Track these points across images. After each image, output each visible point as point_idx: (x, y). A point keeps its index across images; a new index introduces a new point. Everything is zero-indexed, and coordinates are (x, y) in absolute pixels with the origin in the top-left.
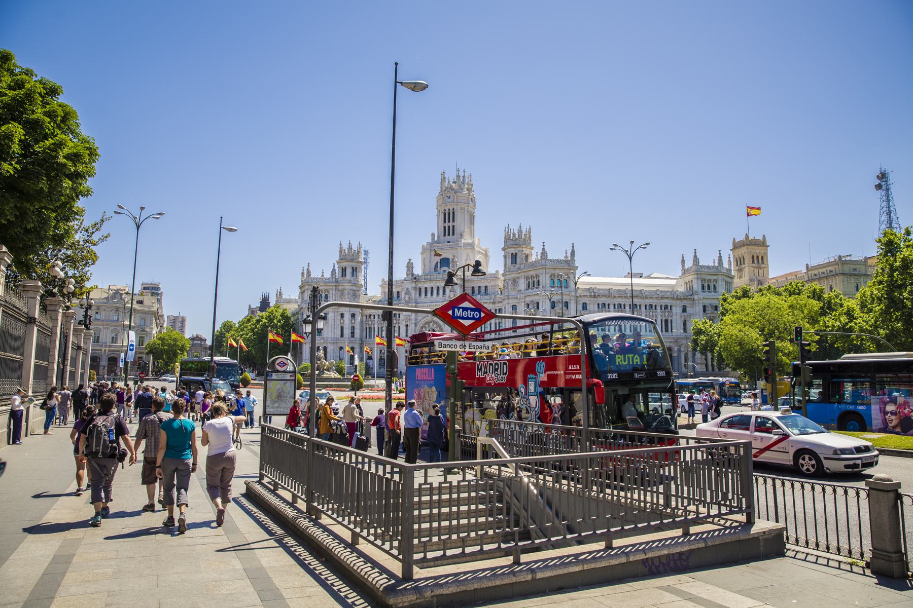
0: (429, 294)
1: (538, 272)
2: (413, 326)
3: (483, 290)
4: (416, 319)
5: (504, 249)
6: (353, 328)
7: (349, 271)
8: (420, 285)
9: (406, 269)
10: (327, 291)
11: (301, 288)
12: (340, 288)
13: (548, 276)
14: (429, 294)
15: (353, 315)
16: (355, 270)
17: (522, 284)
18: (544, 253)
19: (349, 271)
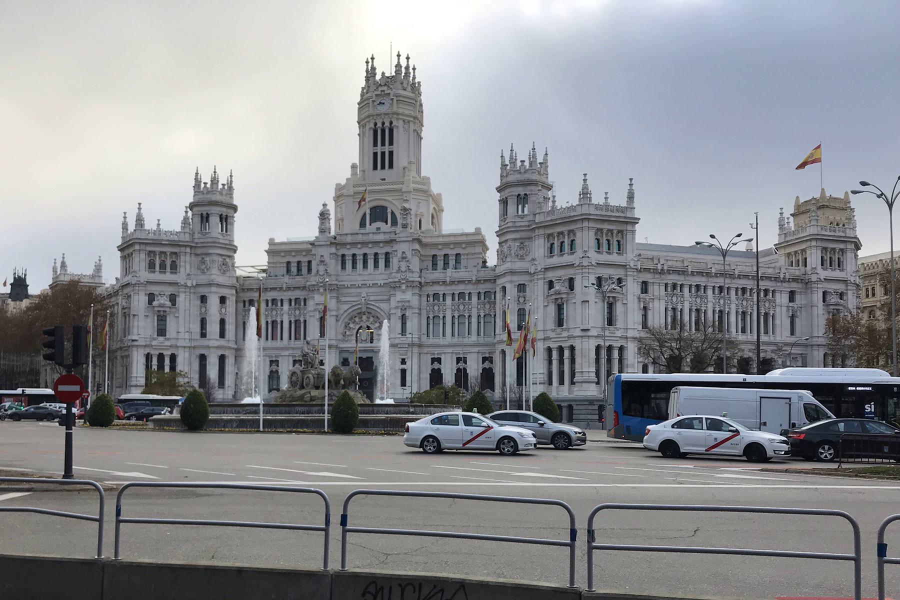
0: (360, 265)
1: (572, 227)
2: (333, 319)
3: (452, 262)
4: (338, 309)
5: (499, 190)
6: (222, 322)
7: (215, 220)
8: (343, 251)
9: (317, 222)
11: (121, 249)
12: (199, 251)
13: (592, 234)
14: (360, 265)
15: (223, 300)
16: (226, 221)
17: (539, 247)
18: (585, 194)
19: (215, 220)
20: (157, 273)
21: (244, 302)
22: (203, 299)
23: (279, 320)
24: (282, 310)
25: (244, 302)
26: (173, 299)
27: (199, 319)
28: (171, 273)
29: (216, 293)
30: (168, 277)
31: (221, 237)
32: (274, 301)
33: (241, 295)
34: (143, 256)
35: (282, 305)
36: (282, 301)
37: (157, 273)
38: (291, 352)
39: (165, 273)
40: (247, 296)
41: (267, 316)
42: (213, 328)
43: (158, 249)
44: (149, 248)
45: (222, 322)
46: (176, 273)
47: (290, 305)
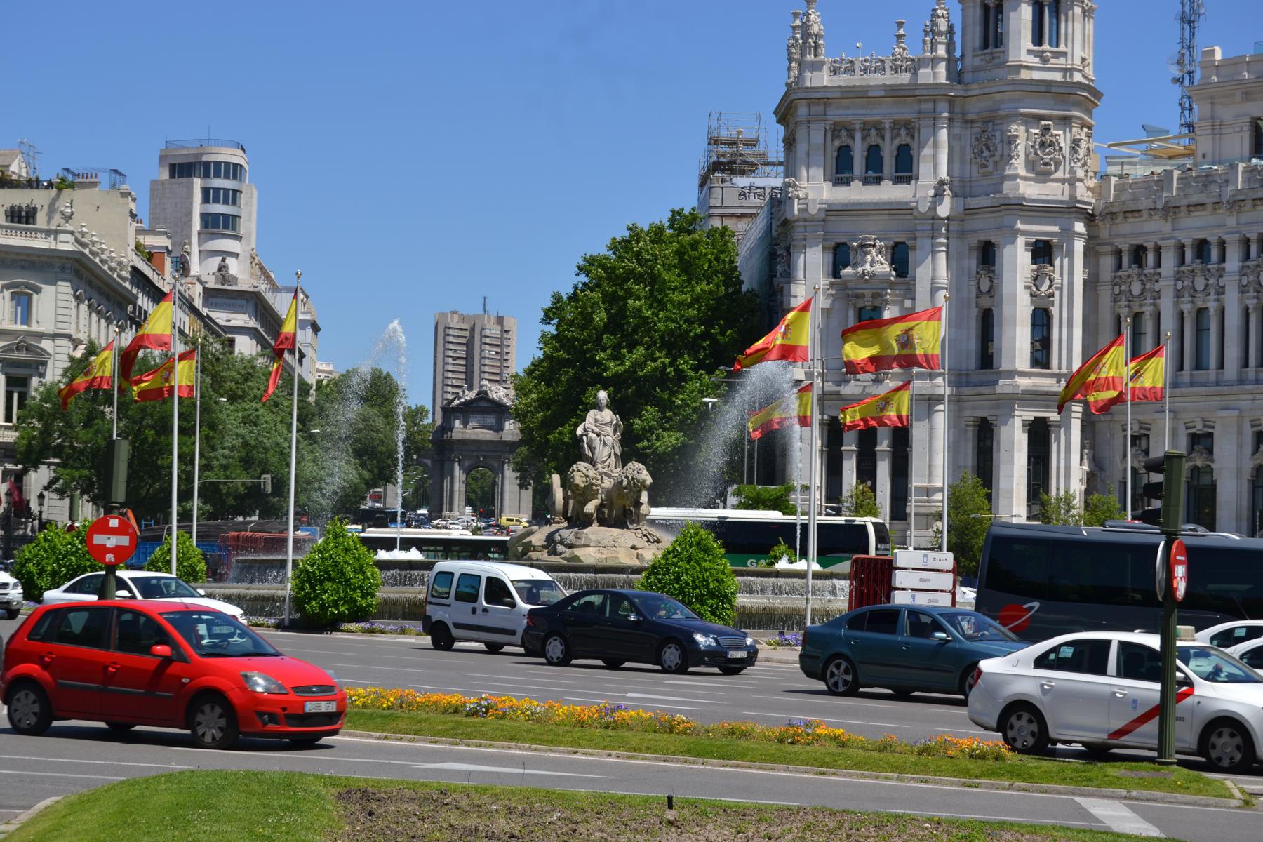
10: (909, 127)
20: (856, 184)
21: (1118, 253)
22: (987, 255)
23: (1212, 306)
24: (1221, 272)
25: (1118, 253)
26: (900, 258)
27: (974, 312)
28: (897, 181)
29: (1025, 233)
30: (888, 192)
31: (1034, 61)
32: (1202, 248)
33: (1104, 231)
34: (817, 136)
35: (1223, 259)
36: (1222, 244)
37: (856, 184)
38: (1245, 402)
39: (877, 181)
40: (1126, 234)
41: (1178, 294)
42: (1017, 342)
43: (855, 115)
44: (838, 114)
45: (1041, 320)
46: (907, 180)
47: (1247, 256)
